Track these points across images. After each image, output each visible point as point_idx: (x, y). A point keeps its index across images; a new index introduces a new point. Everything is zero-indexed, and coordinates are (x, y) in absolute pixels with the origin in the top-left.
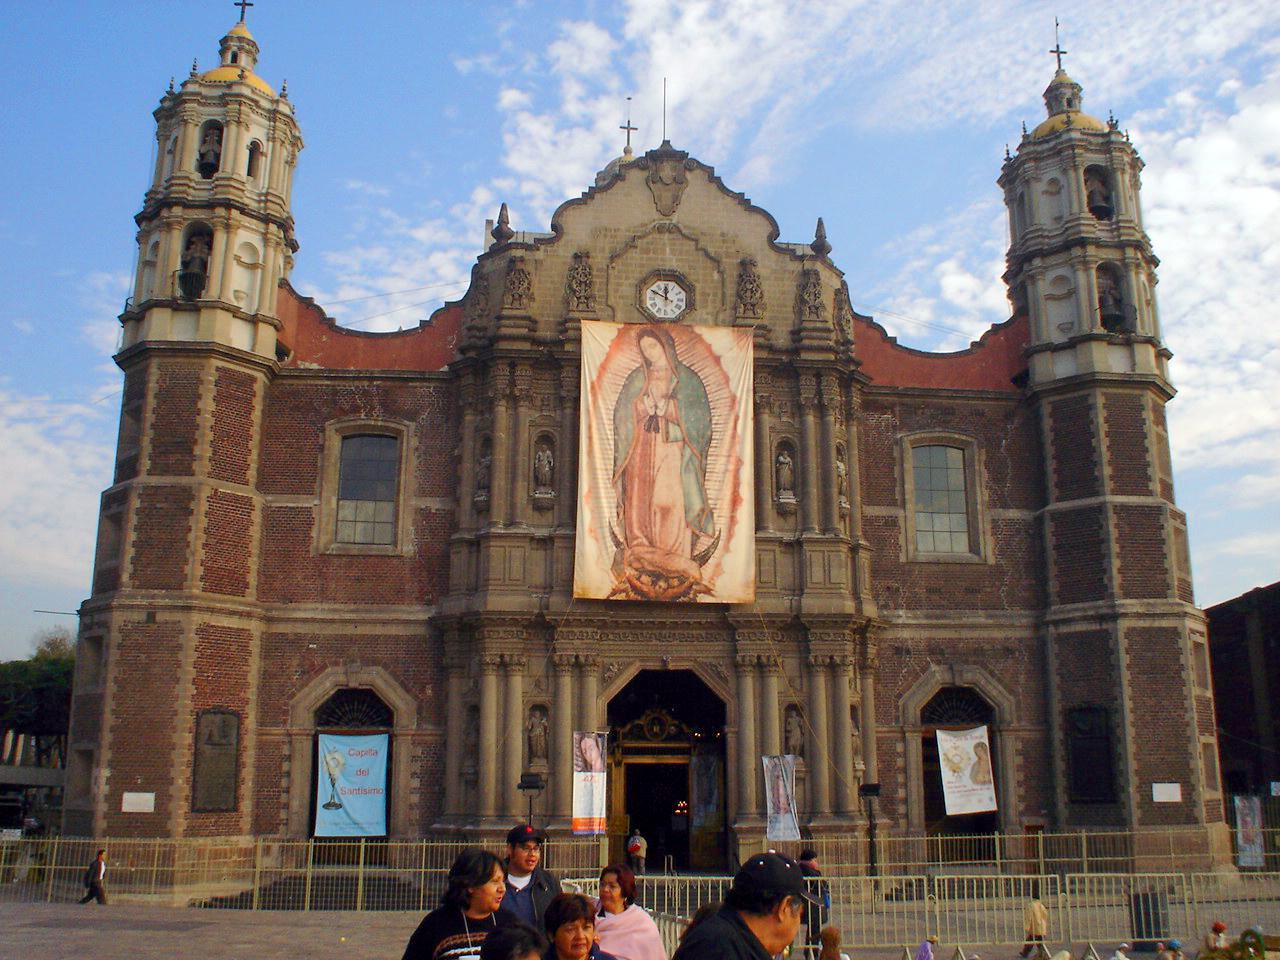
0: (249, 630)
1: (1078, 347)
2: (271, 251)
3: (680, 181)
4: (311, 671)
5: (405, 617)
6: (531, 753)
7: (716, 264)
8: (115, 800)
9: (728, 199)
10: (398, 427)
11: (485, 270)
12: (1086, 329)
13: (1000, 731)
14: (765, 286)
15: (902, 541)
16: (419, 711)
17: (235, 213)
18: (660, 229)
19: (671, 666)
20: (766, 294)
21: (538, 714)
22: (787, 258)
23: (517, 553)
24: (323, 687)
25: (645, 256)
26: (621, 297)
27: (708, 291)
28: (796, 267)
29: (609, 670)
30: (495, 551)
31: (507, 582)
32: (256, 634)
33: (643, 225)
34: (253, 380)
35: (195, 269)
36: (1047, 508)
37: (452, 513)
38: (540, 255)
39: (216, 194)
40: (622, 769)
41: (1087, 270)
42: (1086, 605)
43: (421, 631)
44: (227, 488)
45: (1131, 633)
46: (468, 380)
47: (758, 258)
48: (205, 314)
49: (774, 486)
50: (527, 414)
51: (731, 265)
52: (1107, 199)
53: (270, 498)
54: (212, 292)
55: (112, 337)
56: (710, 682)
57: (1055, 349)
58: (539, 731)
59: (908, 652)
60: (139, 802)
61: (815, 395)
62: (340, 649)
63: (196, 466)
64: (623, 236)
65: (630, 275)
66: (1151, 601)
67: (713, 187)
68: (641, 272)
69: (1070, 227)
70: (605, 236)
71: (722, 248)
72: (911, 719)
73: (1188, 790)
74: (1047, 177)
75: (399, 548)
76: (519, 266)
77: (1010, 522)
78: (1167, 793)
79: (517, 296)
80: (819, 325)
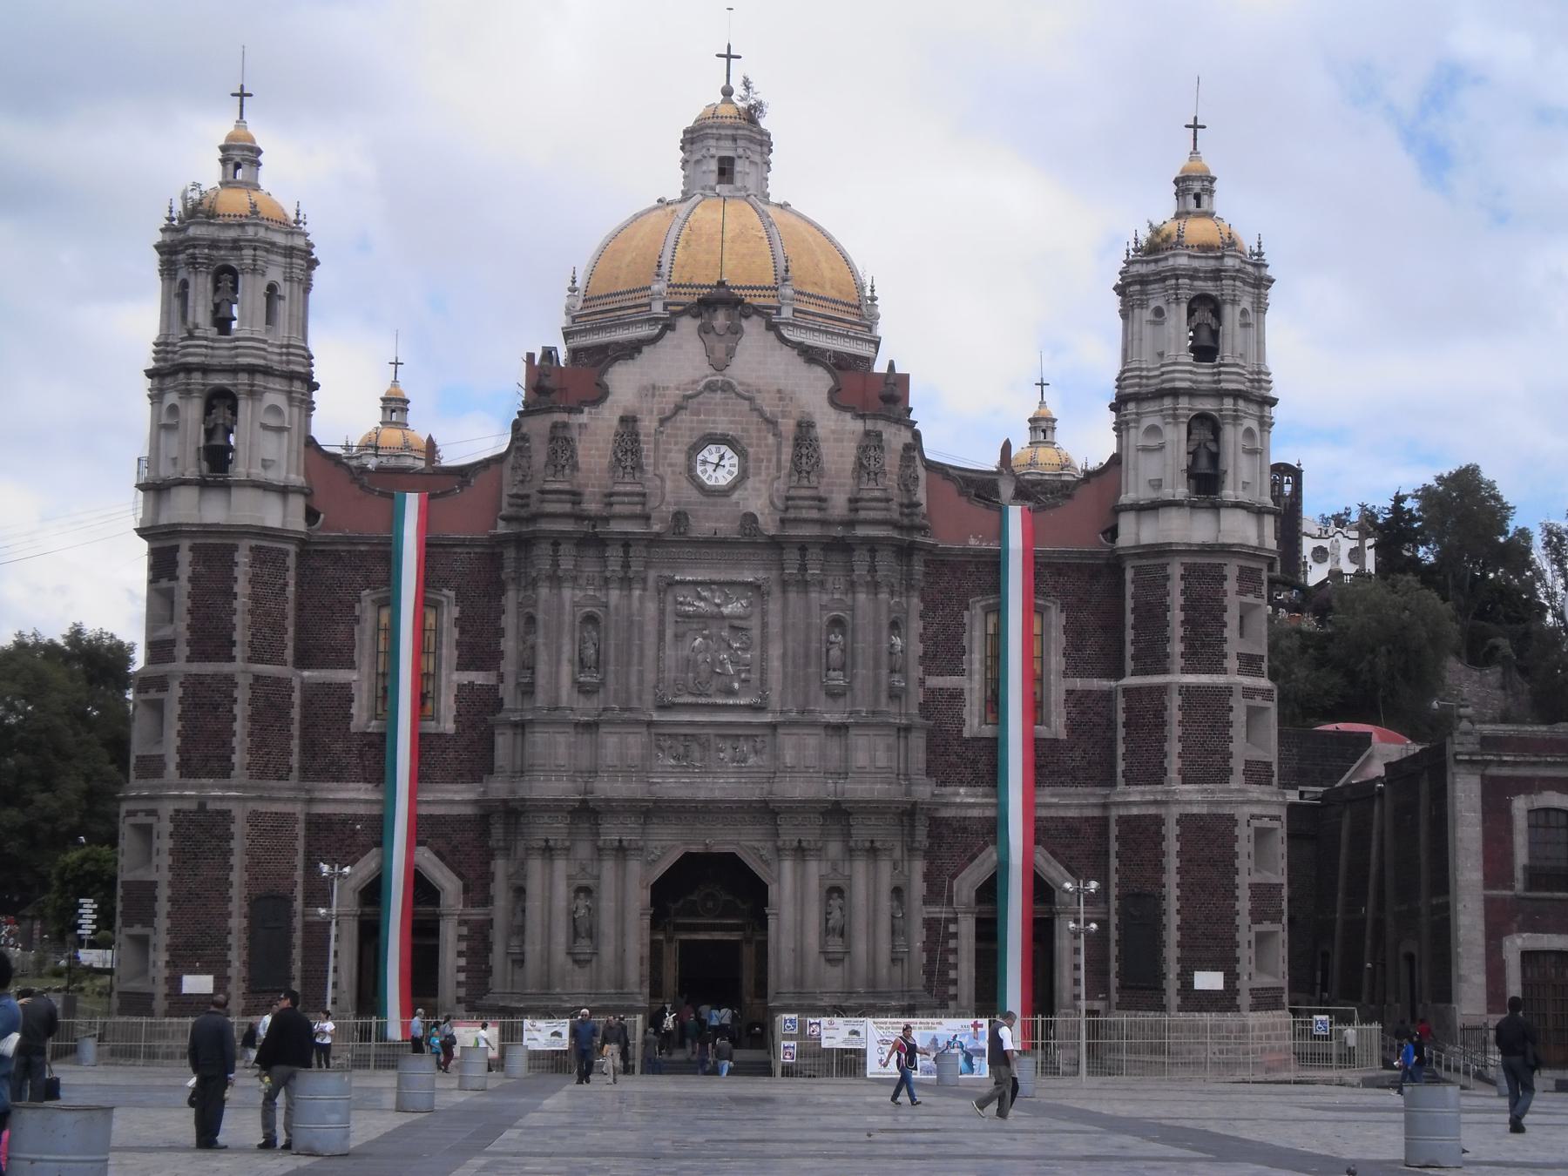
0: (294, 814)
1: (1160, 510)
2: (296, 411)
3: (736, 331)
5: (448, 796)
6: (575, 933)
7: (771, 426)
8: (175, 982)
9: (786, 349)
10: (439, 598)
11: (524, 430)
12: (1167, 493)
13: (1059, 913)
14: (825, 448)
15: (966, 715)
16: (466, 890)
17: (259, 380)
18: (711, 387)
19: (716, 849)
20: (824, 458)
21: (582, 895)
22: (848, 416)
23: (561, 739)
25: (695, 418)
26: (670, 465)
27: (762, 456)
28: (858, 426)
29: (653, 853)
30: (539, 738)
31: (554, 768)
32: (302, 817)
33: (695, 382)
34: (287, 554)
35: (218, 441)
36: (1120, 682)
37: (495, 688)
38: (583, 418)
39: (237, 356)
40: (676, 945)
41: (1176, 424)
42: (1148, 788)
43: (468, 810)
45: (1184, 820)
46: (510, 554)
47: (817, 418)
48: (236, 494)
49: (824, 666)
50: (567, 593)
51: (788, 426)
52: (1215, 334)
53: (306, 673)
54: (239, 470)
55: (129, 508)
57: (1140, 509)
58: (582, 912)
59: (965, 830)
60: (198, 984)
61: (869, 571)
63: (237, 651)
64: (673, 397)
65: (680, 439)
66: (1211, 786)
67: (772, 335)
68: (691, 437)
69: (1168, 372)
70: (653, 396)
71: (778, 406)
72: (965, 899)
73: (1231, 978)
74: (1153, 304)
75: (442, 725)
76: (560, 433)
78: (1209, 981)
79: (559, 468)
80: (877, 494)
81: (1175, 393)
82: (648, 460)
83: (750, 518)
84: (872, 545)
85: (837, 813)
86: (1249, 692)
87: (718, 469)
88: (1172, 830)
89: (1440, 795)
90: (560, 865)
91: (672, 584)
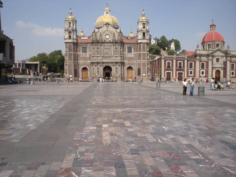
3: (108, 26)
4: (81, 66)
8: (69, 76)
24: (82, 67)
35: (70, 35)
44: (74, 53)
51: (113, 34)
56: (111, 67)
57: (139, 40)
60: (71, 76)
62: (83, 64)
64: (104, 31)
77: (135, 54)
78: (144, 75)
81: (142, 31)
82: (102, 36)
83: (110, 40)
84: (119, 43)
85: (117, 63)
86: (147, 53)
87: (107, 37)
88: (141, 64)
89: (161, 61)
90: (96, 67)
91: (104, 46)
